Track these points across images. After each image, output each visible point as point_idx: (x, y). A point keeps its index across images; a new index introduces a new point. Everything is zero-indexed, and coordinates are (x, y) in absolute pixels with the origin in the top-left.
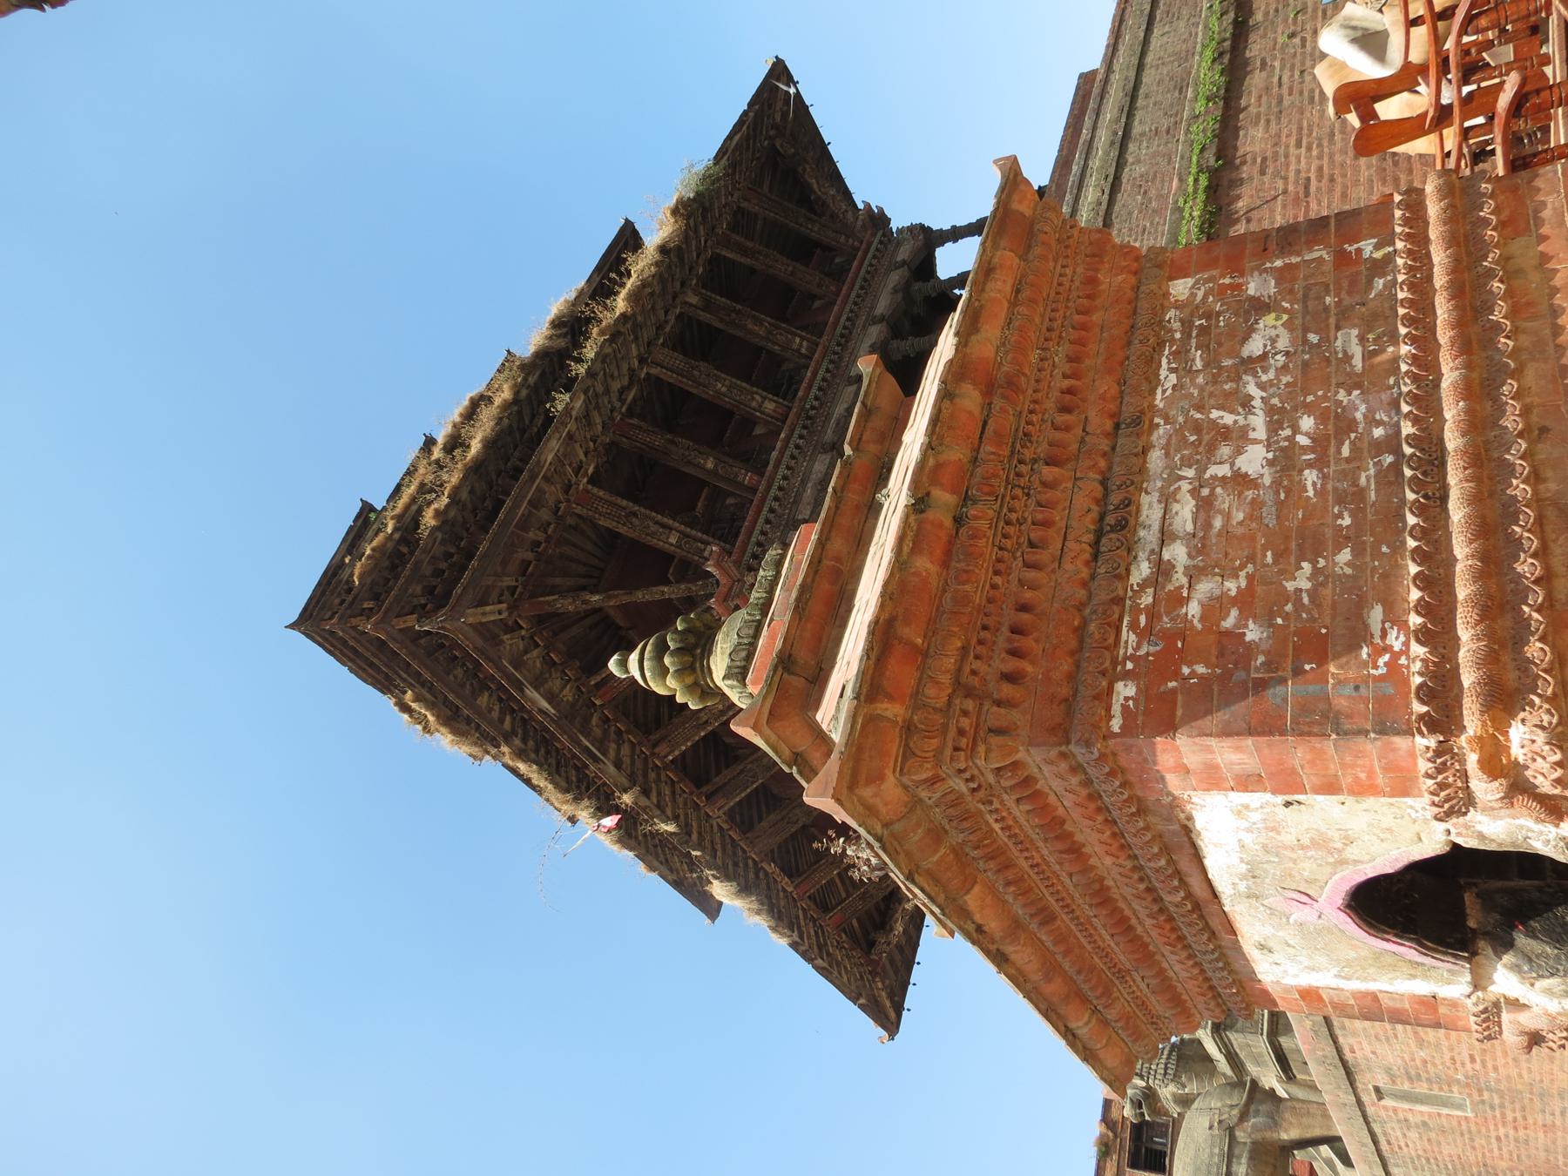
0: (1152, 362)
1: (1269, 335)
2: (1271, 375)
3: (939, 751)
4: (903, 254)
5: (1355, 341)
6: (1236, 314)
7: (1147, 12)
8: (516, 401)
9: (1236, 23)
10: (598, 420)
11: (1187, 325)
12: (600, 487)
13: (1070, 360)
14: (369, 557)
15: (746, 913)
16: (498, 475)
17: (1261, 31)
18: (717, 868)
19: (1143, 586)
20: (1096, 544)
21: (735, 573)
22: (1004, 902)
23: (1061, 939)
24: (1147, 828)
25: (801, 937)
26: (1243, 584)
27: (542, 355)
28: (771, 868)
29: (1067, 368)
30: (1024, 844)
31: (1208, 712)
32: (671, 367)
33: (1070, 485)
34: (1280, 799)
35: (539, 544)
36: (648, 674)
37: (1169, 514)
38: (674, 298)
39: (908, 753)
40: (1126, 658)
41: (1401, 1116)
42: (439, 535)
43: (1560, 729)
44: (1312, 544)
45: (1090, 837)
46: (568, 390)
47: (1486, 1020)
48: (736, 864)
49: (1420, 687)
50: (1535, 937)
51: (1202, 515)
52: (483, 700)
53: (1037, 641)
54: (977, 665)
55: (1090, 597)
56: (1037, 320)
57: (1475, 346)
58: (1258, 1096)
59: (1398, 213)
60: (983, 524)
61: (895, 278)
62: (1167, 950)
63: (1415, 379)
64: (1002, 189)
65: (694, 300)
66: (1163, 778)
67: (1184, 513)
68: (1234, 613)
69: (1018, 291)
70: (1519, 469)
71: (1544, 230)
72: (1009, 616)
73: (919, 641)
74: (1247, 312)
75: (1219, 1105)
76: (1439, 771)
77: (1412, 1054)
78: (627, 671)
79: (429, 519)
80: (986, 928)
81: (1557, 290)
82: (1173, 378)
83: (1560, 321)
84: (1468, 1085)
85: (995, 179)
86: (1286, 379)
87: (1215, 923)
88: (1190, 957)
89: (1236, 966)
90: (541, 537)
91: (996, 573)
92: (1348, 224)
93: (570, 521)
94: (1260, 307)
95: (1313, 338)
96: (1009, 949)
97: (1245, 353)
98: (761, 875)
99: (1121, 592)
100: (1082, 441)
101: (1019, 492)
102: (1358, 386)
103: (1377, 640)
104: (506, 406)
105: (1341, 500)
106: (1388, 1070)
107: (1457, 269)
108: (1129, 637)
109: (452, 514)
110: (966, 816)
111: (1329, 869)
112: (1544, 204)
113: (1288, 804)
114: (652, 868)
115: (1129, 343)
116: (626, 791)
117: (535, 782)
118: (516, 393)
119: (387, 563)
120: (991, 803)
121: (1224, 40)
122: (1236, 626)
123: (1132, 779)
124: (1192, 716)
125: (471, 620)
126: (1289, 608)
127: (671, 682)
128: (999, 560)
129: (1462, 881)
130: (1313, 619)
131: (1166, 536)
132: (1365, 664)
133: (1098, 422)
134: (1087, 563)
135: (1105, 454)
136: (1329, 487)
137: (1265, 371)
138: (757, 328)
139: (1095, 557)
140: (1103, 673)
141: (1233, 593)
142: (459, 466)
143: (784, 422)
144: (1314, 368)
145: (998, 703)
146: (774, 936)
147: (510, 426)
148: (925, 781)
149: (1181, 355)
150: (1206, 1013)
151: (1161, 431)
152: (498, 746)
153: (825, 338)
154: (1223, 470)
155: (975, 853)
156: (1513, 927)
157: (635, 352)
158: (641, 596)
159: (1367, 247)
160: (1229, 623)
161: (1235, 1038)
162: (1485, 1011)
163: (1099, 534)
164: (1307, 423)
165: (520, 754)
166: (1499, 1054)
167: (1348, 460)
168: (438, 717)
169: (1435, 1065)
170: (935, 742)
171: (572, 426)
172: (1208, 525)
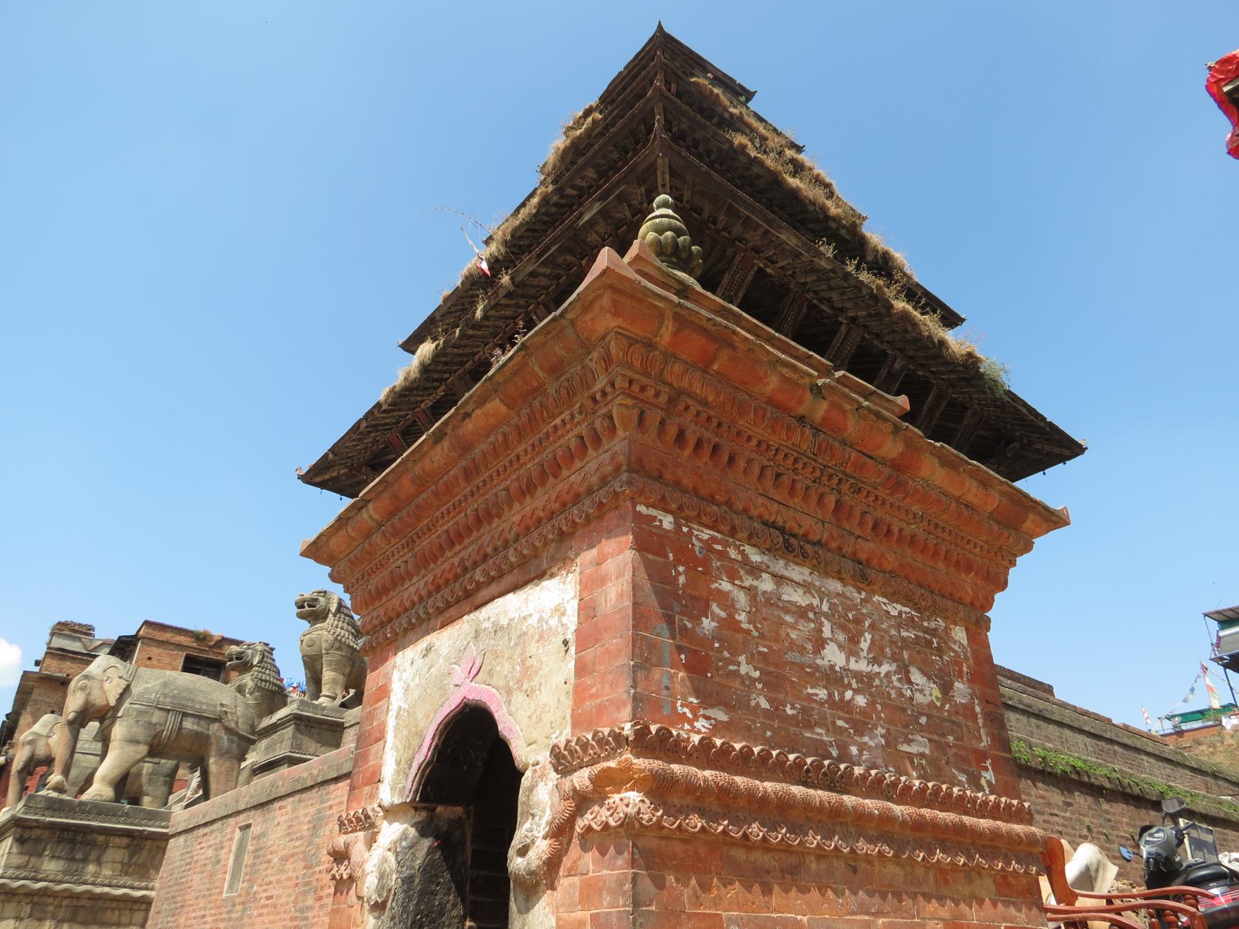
0: (907, 600)
1: (925, 690)
2: (897, 684)
3: (630, 366)
5: (921, 750)
6: (940, 670)
7: (1104, 735)
8: (828, 218)
9: (1101, 788)
10: (809, 280)
11: (934, 632)
12: (755, 278)
13: (913, 537)
14: (711, 91)
15: (406, 369)
16: (769, 200)
17: (1093, 806)
18: (444, 348)
19: (742, 553)
20: (773, 525)
22: (487, 437)
23: (449, 489)
24: (546, 544)
25: (385, 411)
26: (745, 626)
27: (862, 242)
28: (440, 393)
29: (907, 532)
30: (537, 448)
31: (651, 578)
33: (819, 516)
34: (570, 636)
35: (715, 224)
36: (657, 220)
37: (798, 586)
38: (901, 350)
39: (632, 341)
40: (691, 528)
41: (226, 844)
42: (726, 147)
43: (637, 825)
44: (773, 682)
45: (540, 501)
46: (835, 257)
47: (358, 820)
48: (446, 364)
49: (671, 733)
50: (428, 854)
51: (794, 609)
52: (591, 173)
53: (706, 464)
54: (693, 410)
55: (736, 512)
56: (944, 517)
57: (918, 834)
58: (244, 744)
59: (1015, 802)
60: (797, 438)
62: (430, 578)
63: (894, 784)
64: (1046, 508)
65: (897, 366)
66: (593, 547)
67: (797, 597)
68: (723, 614)
69: (967, 506)
70: (828, 843)
71: (1000, 905)
72: (727, 446)
73: (715, 367)
74: (941, 678)
75: (239, 714)
76: (602, 742)
77: (276, 852)
78: (658, 207)
79: (739, 139)
80: (467, 420)
81: (957, 905)
82: (894, 613)
83: (934, 901)
84: (248, 894)
85: (1055, 504)
86: (893, 692)
87: (453, 611)
88: (421, 598)
89: (411, 635)
90: (720, 225)
91: (759, 443)
93: (730, 252)
94: (946, 688)
95: (923, 720)
96: (446, 443)
97: (913, 669)
98: (435, 384)
99: (740, 535)
100: (851, 533)
101: (818, 474)
102: (888, 744)
103: (702, 712)
104: (824, 209)
105: (804, 710)
106: (263, 834)
107: (975, 833)
108: (706, 534)
109: (743, 159)
110: (571, 393)
111: (502, 683)
112: (1020, 911)
113: (566, 643)
114: (446, 300)
115: (921, 586)
116: (512, 279)
117: (523, 210)
118: (834, 219)
119: (705, 105)
120: (580, 413)
121: (1089, 777)
122: (713, 613)
123: (592, 526)
124: (648, 565)
125: (659, 161)
126: (726, 654)
127: (651, 236)
128: (769, 446)
129: (471, 808)
130: (718, 669)
131: (779, 579)
132: (684, 699)
133: (867, 548)
134: (760, 516)
135: (840, 549)
136: (814, 705)
137: (900, 680)
139: (765, 523)
140: (680, 508)
141: (737, 617)
142: (780, 168)
144: (903, 718)
145: (662, 423)
146: (386, 390)
147: (808, 212)
148: (608, 353)
149: (911, 623)
150: (368, 619)
151: (856, 595)
152: (554, 182)
154: (827, 632)
155: (537, 403)
156: (436, 838)
157: (860, 313)
159: (989, 776)
160: (715, 607)
161: (289, 731)
162: (367, 817)
163: (782, 530)
164: (861, 701)
165: (545, 200)
166: (272, 918)
167: (834, 723)
168: (579, 138)
169: (266, 869)
170: (637, 364)
171: (806, 257)
172: (788, 612)
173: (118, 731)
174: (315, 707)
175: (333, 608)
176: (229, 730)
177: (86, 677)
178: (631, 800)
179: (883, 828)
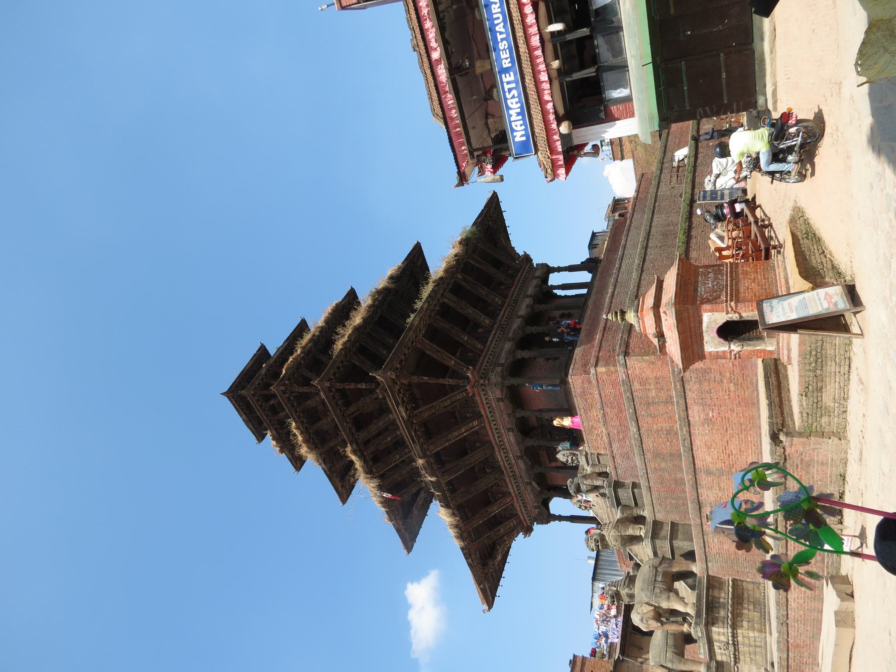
1: (711, 275)
4: (538, 273)
21: (477, 378)
32: (451, 300)
37: (701, 290)
44: (716, 291)
45: (692, 320)
61: (535, 282)
65: (460, 277)
79: (339, 345)
92: (720, 265)
114: (391, 520)
116: (421, 458)
138: (483, 292)
143: (492, 327)
144: (716, 278)
153: (508, 300)
158: (441, 381)
173: (665, 605)
174: (646, 534)
175: (599, 531)
176: (660, 564)
177: (642, 620)
178: (733, 304)
179: (731, 281)
